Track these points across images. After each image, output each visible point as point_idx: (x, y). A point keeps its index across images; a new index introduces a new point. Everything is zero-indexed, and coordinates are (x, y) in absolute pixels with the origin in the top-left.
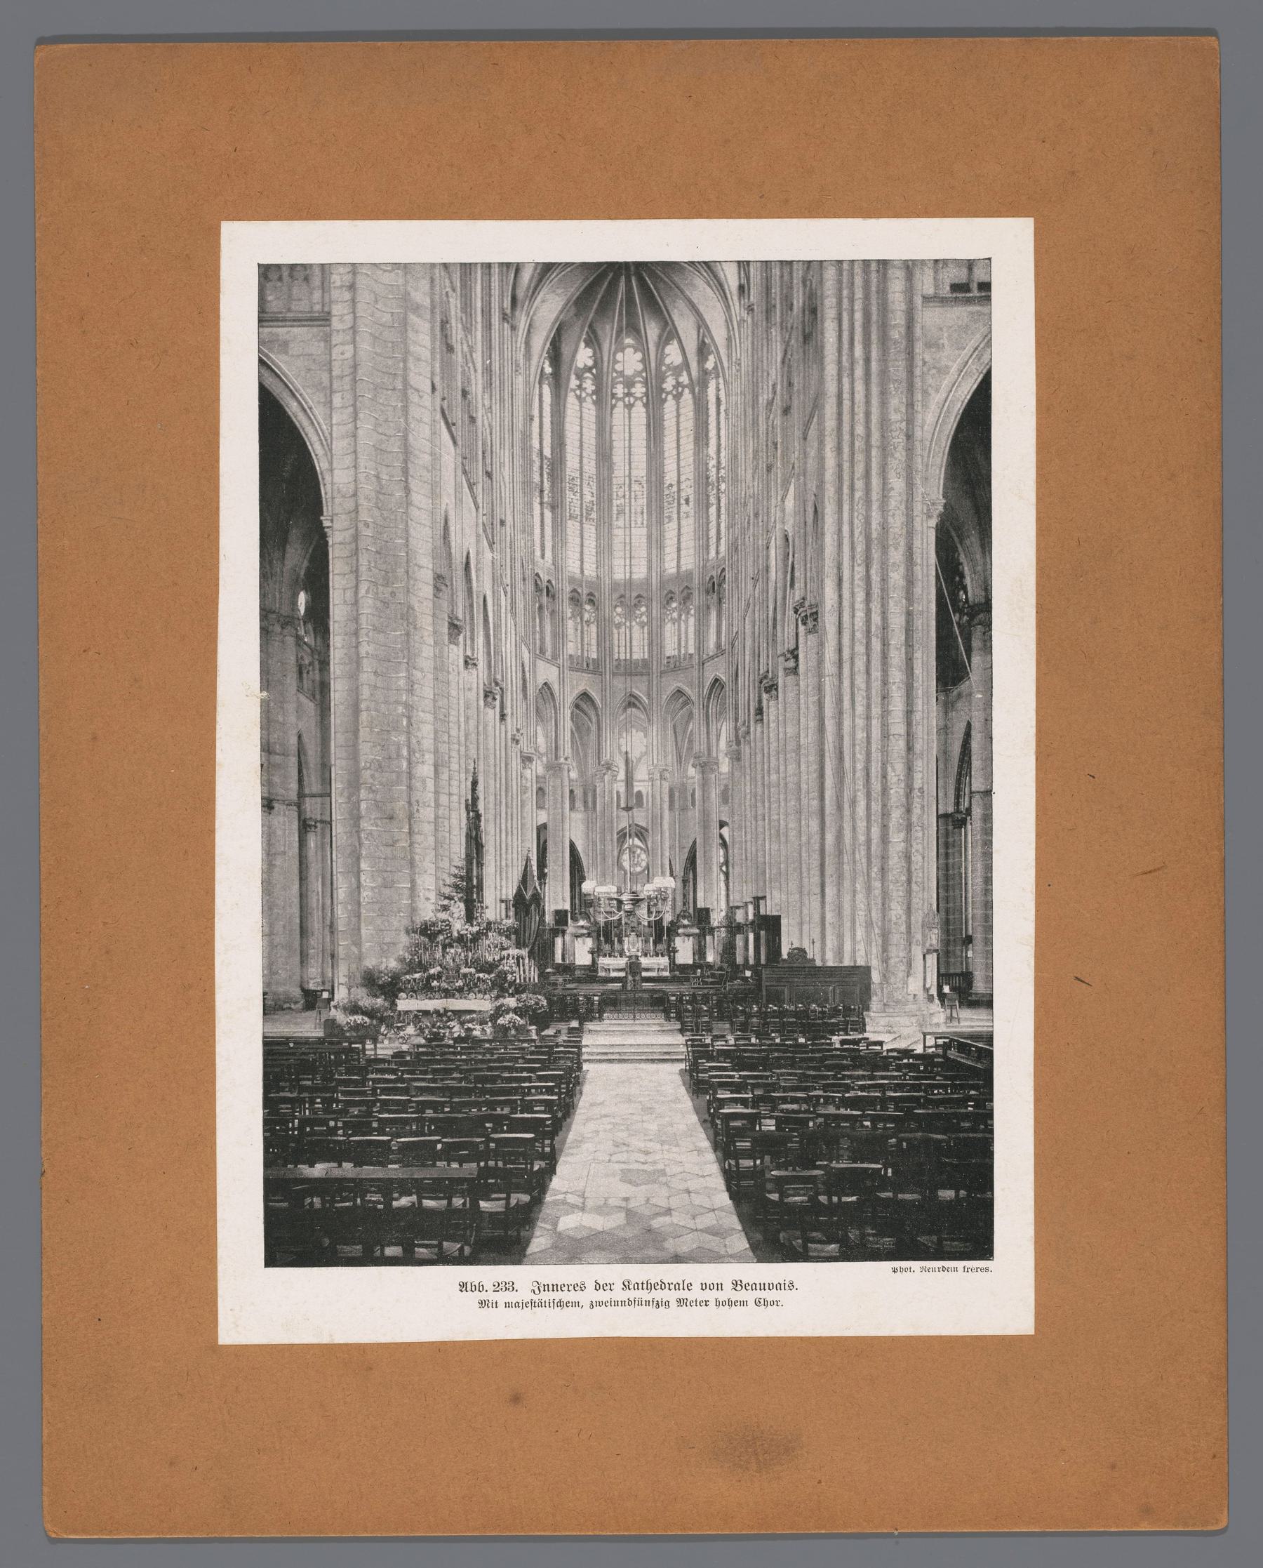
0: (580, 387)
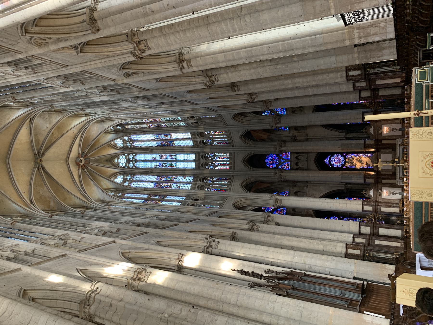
0: (128, 181)
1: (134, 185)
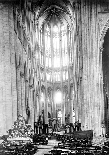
0: (47, 34)
1: (46, 37)
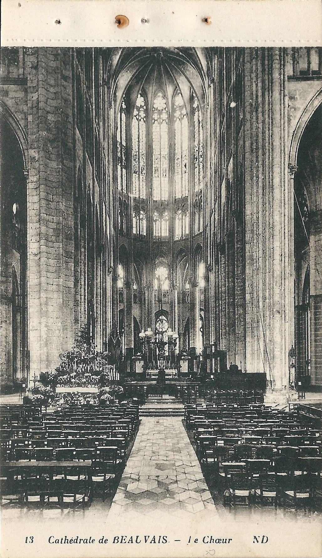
1: (134, 122)
